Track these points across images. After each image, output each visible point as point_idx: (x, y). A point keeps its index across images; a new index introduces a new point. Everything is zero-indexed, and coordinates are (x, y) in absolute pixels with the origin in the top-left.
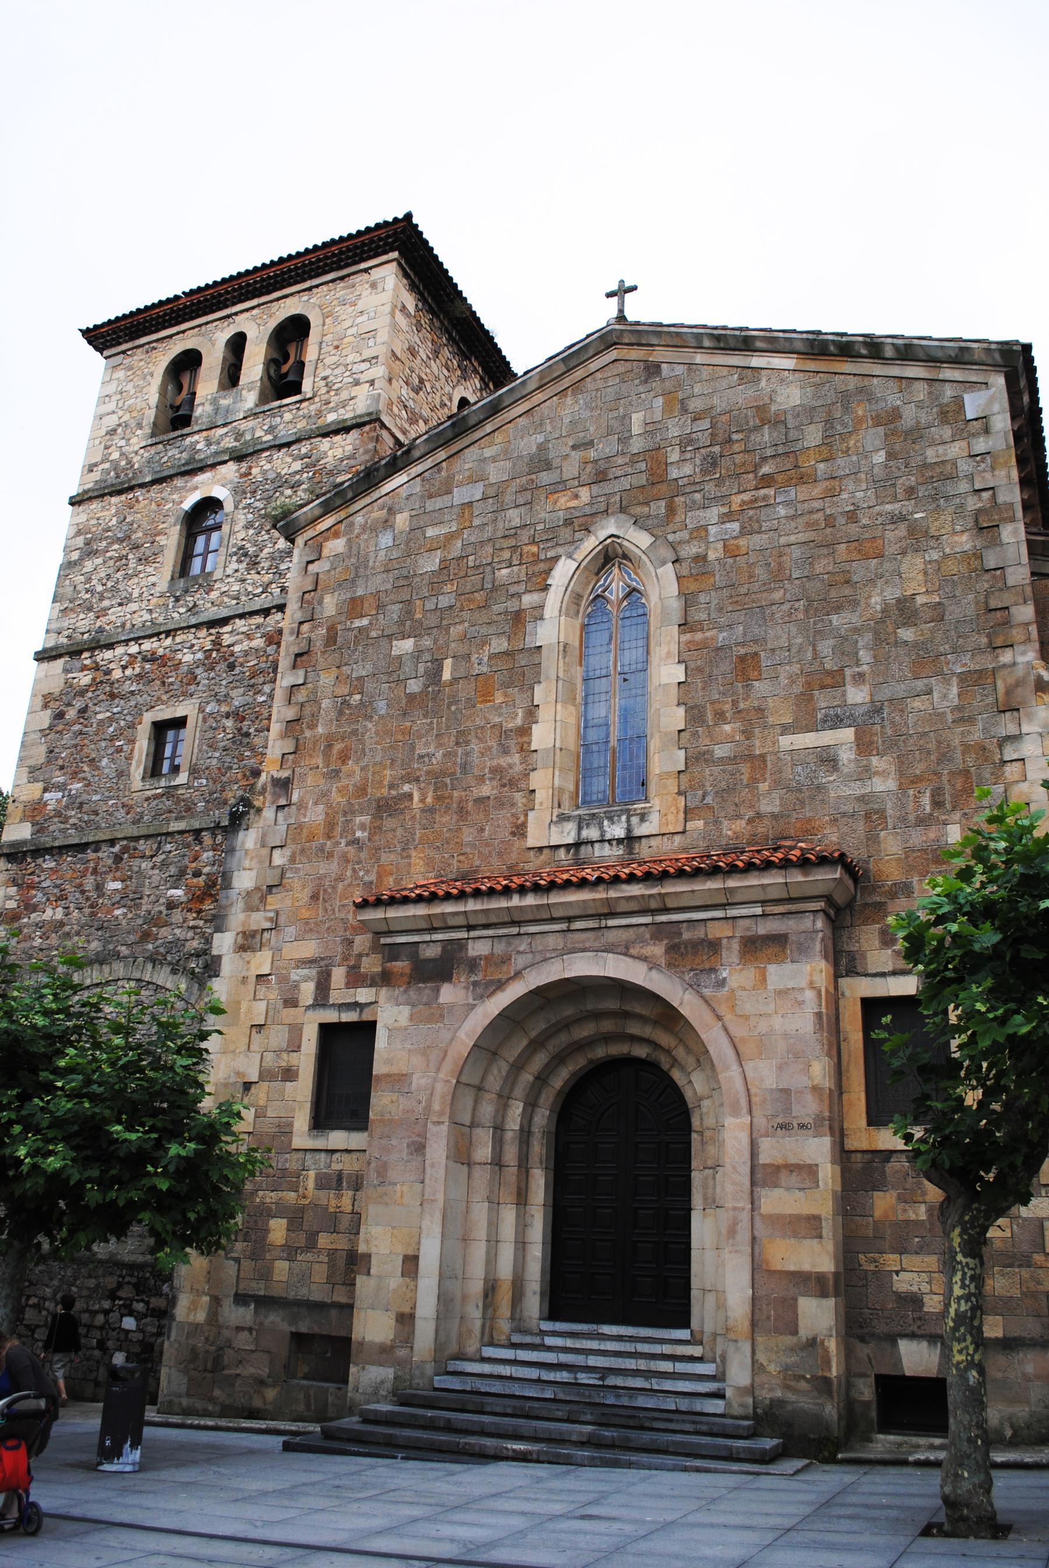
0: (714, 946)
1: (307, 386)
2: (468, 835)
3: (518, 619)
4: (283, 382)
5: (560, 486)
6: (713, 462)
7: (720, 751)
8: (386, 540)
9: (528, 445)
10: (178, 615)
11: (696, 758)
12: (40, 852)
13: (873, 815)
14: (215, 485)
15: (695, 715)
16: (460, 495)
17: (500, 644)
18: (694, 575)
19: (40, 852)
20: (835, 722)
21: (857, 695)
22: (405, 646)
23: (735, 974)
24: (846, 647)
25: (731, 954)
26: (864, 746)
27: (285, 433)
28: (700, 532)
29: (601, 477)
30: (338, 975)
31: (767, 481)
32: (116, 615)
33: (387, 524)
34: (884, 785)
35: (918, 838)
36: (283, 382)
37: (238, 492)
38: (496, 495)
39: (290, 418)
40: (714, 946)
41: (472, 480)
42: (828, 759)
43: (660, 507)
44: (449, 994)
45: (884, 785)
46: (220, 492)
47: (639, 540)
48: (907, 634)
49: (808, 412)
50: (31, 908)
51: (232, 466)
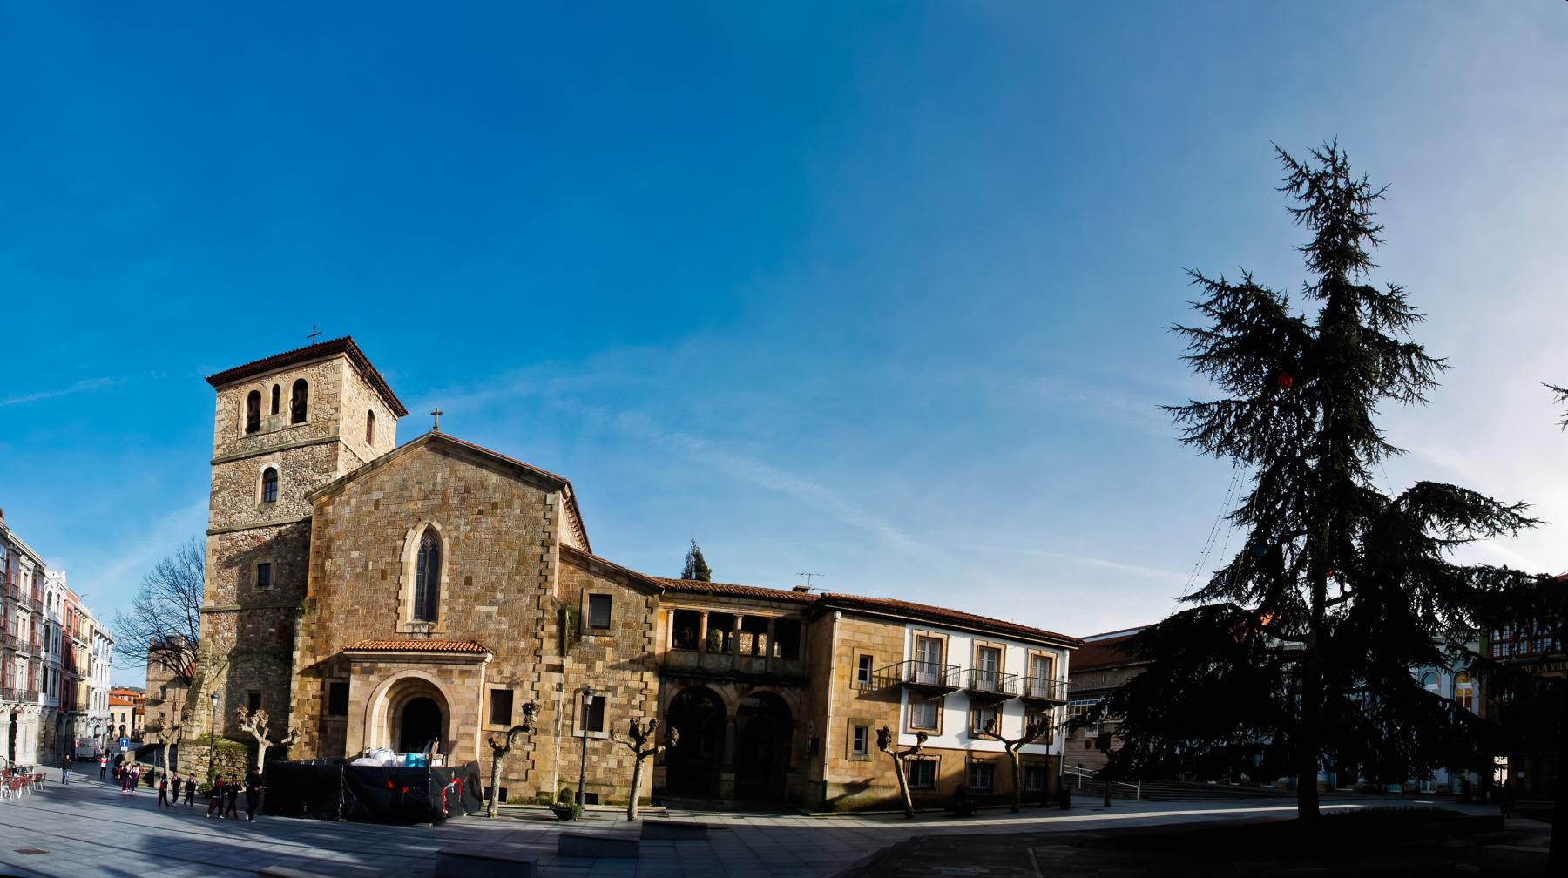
0: (451, 672)
1: (309, 417)
2: (377, 626)
3: (397, 551)
4: (299, 414)
5: (410, 499)
6: (463, 501)
7: (459, 608)
8: (347, 509)
9: (400, 478)
10: (262, 520)
11: (452, 609)
12: (219, 612)
13: (500, 634)
14: (274, 461)
15: (452, 595)
16: (377, 495)
17: (389, 559)
18: (455, 543)
19: (219, 612)
20: (492, 604)
21: (500, 596)
22: (355, 554)
23: (457, 680)
24: (499, 579)
25: (456, 674)
26: (500, 613)
27: (300, 441)
28: (457, 528)
29: (426, 498)
30: (336, 668)
31: (481, 512)
32: (237, 517)
33: (348, 502)
34: (504, 627)
35: (511, 644)
36: (299, 414)
37: (284, 466)
38: (387, 497)
39: (302, 435)
40: (451, 672)
41: (381, 489)
42: (489, 616)
43: (444, 515)
44: (373, 678)
45: (504, 627)
46: (275, 466)
47: (438, 527)
48: (518, 578)
49: (496, 487)
50: (217, 632)
51: (278, 455)
